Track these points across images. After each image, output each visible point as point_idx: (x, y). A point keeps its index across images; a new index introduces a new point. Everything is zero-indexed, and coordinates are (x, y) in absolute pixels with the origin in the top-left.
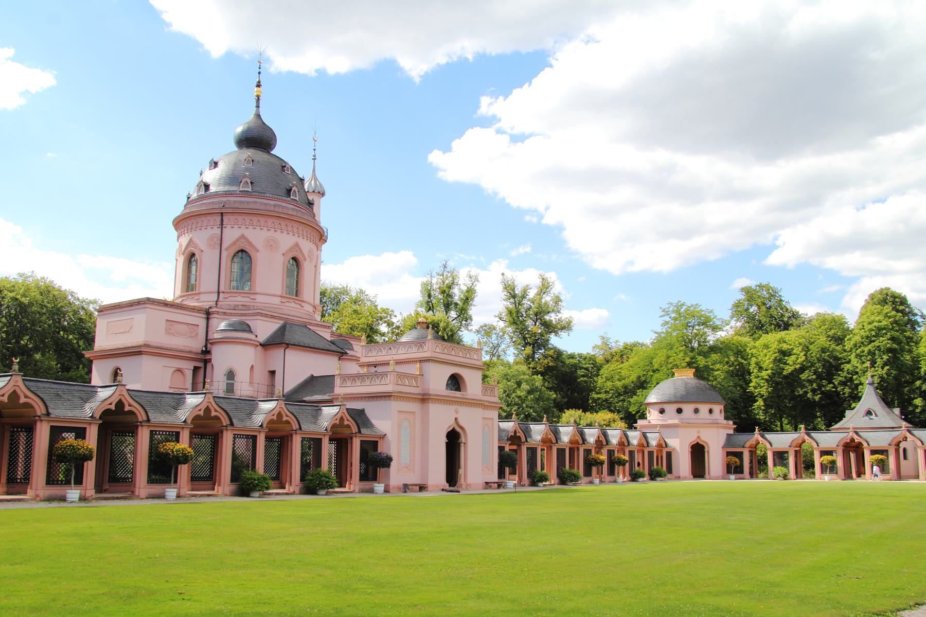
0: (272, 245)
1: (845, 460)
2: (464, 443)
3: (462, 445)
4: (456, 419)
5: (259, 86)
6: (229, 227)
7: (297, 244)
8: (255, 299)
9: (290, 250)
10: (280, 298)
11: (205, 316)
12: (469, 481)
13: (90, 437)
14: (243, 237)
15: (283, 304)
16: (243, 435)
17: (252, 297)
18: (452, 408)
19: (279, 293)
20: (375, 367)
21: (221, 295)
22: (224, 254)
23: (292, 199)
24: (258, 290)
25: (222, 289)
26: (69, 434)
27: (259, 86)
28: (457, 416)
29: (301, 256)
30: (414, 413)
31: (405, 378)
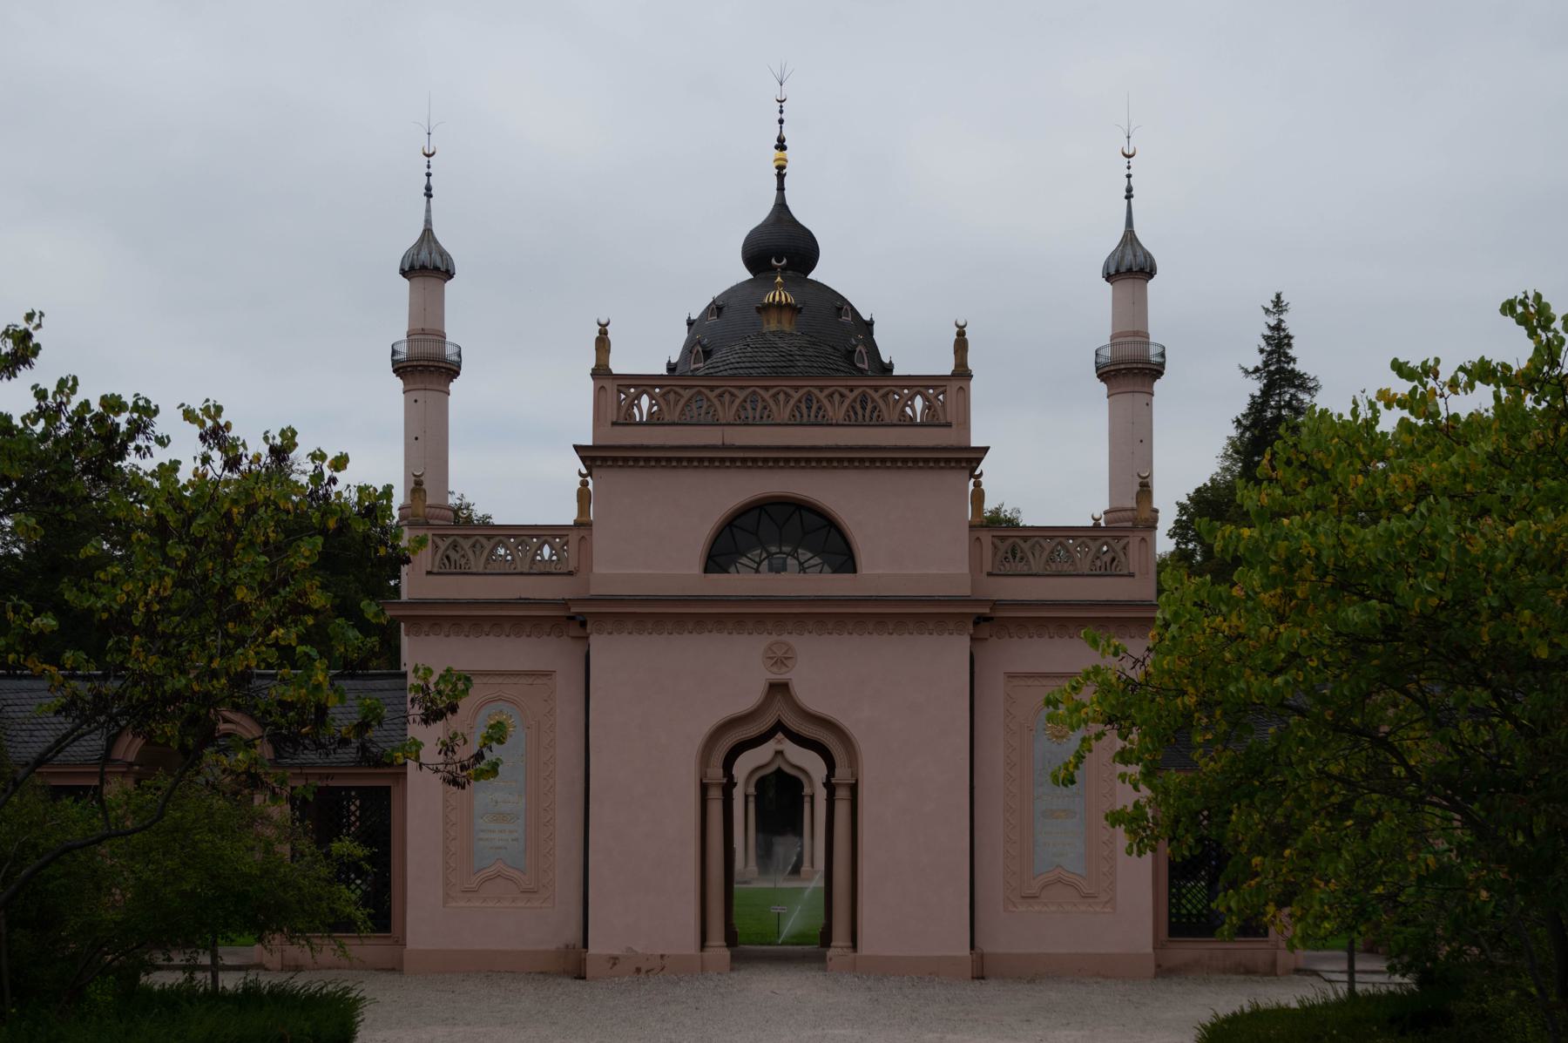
5: (781, 145)
27: (781, 145)
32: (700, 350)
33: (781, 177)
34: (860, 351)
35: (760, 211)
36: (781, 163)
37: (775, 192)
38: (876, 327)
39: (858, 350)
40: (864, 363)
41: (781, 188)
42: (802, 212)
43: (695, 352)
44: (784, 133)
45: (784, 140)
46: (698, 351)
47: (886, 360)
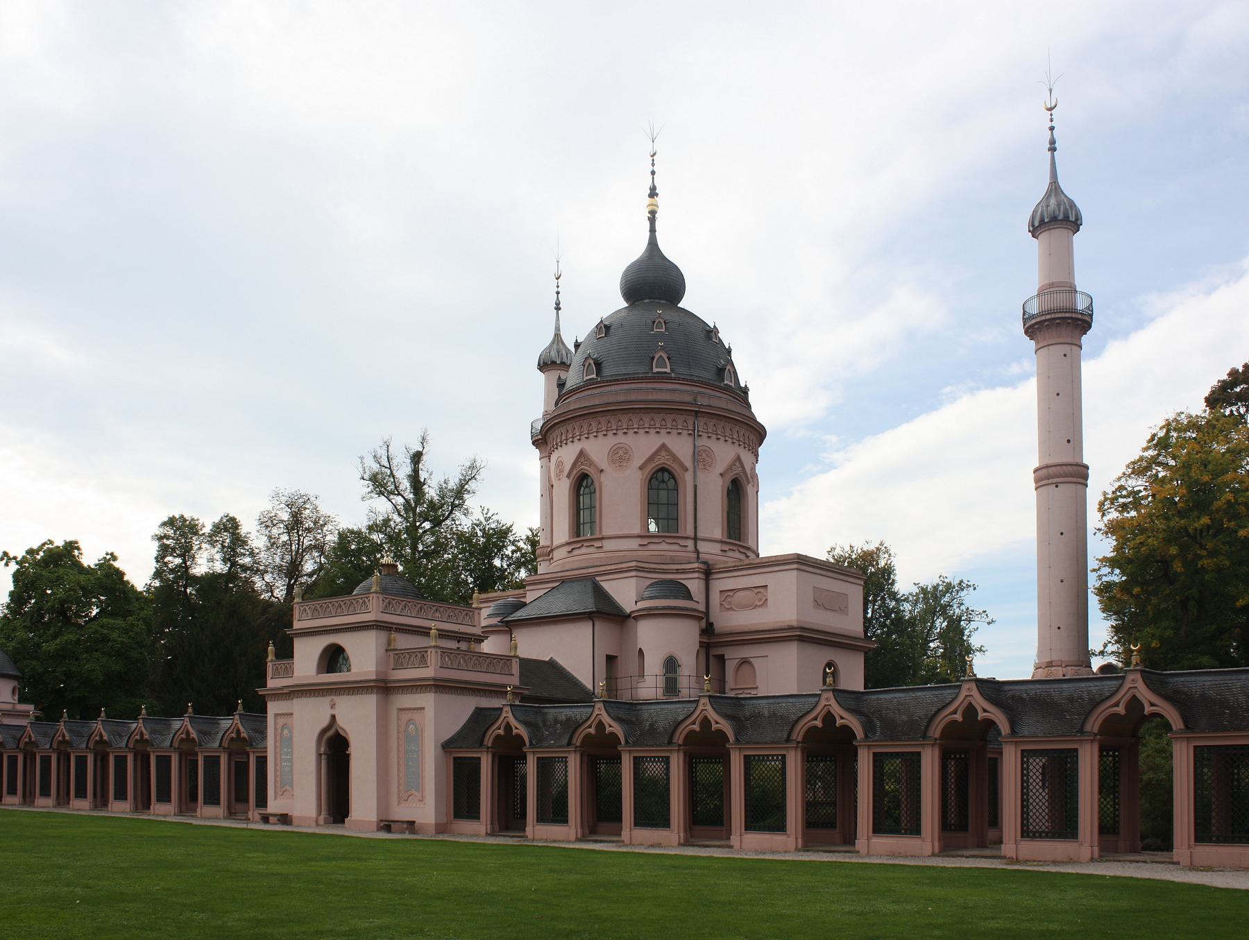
0: (620, 457)
1: (183, 762)
7: (663, 447)
8: (601, 547)
9: (651, 458)
10: (638, 539)
11: (702, 576)
13: (1188, 776)
14: (582, 454)
15: (645, 548)
16: (659, 757)
20: (459, 642)
24: (605, 533)
26: (1040, 777)
29: (675, 466)
31: (459, 657)
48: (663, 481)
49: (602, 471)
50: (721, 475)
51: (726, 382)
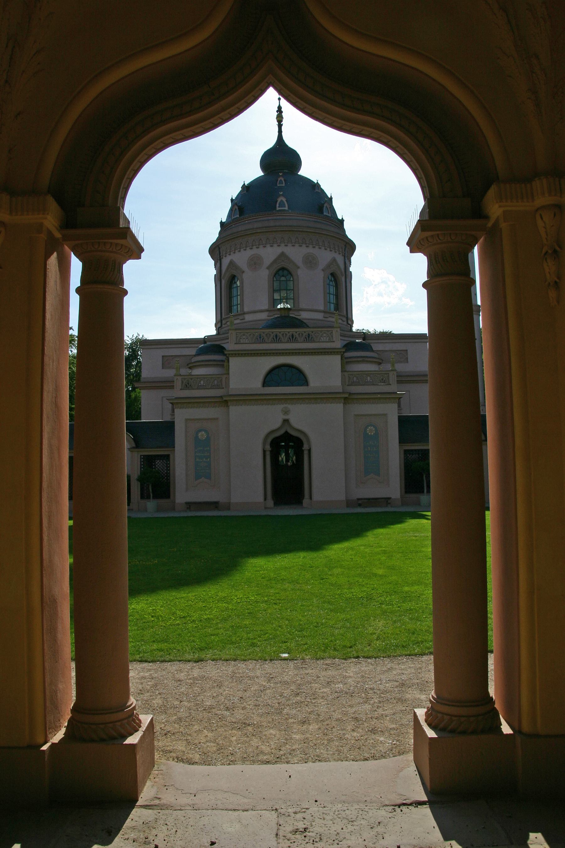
0: (255, 263)
2: (309, 451)
3: (306, 453)
4: (286, 421)
6: (224, 257)
7: (283, 254)
9: (275, 261)
12: (316, 497)
14: (232, 263)
17: (241, 317)
18: (279, 407)
19: (266, 307)
21: (224, 322)
22: (223, 282)
23: (280, 210)
24: (246, 310)
25: (223, 316)
28: (286, 417)
30: (217, 419)
32: (237, 208)
33: (280, 126)
34: (326, 207)
35: (271, 142)
36: (280, 119)
37: (277, 134)
38: (333, 200)
39: (325, 205)
40: (329, 213)
41: (280, 132)
42: (290, 141)
43: (234, 210)
44: (281, 105)
45: (281, 108)
46: (236, 209)
47: (340, 218)
48: (283, 276)
49: (243, 272)
50: (323, 270)
51: (325, 214)
